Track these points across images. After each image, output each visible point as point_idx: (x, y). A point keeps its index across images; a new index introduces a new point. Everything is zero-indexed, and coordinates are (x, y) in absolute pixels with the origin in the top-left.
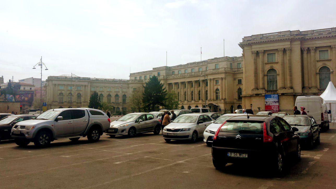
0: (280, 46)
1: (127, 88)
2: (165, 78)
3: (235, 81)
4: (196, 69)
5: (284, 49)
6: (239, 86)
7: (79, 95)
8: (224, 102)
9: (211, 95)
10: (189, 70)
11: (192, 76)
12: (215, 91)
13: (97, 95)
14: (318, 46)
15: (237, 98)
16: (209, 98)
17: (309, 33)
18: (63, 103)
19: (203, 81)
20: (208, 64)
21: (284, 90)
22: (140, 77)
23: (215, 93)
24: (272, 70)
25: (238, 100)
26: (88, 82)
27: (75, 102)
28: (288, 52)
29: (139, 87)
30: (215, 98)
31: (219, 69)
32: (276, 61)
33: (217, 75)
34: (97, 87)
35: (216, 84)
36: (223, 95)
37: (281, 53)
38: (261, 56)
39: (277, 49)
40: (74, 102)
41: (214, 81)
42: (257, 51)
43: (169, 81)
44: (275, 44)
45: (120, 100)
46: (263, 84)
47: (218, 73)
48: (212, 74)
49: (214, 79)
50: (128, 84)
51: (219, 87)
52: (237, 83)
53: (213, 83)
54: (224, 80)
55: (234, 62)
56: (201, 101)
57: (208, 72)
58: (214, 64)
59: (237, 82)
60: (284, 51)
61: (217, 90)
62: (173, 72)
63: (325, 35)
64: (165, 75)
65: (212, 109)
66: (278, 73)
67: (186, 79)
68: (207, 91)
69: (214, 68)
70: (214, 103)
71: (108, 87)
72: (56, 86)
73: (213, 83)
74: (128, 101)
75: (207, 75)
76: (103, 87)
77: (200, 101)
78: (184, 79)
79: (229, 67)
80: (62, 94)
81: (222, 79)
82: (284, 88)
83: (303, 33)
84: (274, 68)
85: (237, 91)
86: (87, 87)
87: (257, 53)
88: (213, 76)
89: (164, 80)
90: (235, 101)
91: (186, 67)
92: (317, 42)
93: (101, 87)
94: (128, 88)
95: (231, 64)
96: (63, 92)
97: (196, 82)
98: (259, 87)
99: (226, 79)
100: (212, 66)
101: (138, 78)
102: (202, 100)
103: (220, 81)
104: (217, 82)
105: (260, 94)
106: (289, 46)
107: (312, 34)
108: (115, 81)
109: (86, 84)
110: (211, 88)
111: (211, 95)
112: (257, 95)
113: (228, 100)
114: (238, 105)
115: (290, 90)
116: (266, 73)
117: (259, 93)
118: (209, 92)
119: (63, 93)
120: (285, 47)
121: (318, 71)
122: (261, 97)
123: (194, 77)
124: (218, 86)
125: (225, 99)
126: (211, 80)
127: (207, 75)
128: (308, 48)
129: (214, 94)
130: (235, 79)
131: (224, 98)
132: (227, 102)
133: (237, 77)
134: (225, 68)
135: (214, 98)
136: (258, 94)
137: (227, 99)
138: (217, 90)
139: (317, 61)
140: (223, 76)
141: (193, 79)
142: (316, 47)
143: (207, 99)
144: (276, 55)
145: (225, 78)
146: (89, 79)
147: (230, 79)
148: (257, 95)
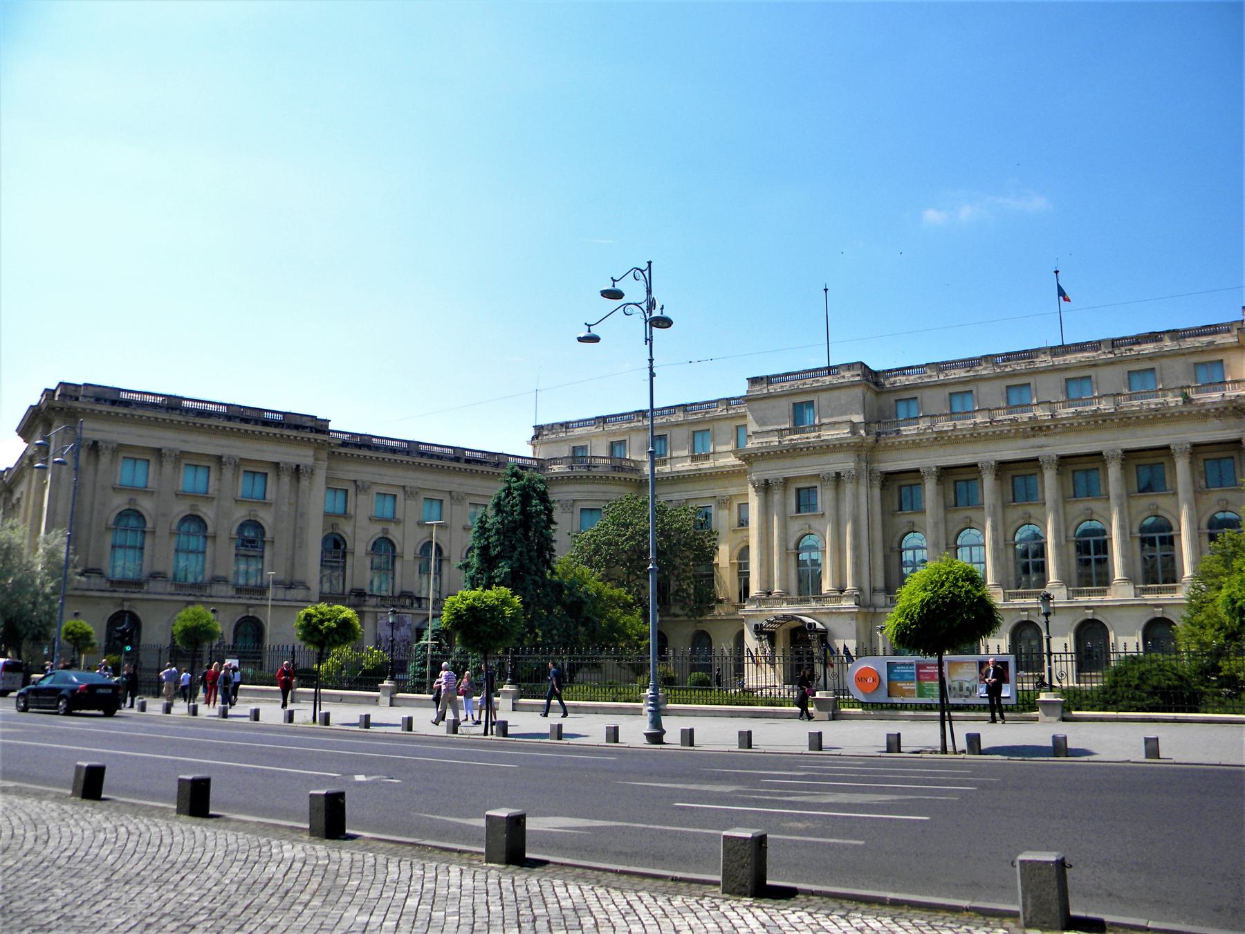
7: (249, 533)
27: (224, 580)
34: (360, 487)
72: (97, 457)
76: (392, 491)
80: (133, 522)
86: (304, 482)
93: (383, 490)
96: (146, 505)
101: (600, 449)
108: (468, 461)
109: (303, 456)
119: (140, 516)
141: (1112, 442)
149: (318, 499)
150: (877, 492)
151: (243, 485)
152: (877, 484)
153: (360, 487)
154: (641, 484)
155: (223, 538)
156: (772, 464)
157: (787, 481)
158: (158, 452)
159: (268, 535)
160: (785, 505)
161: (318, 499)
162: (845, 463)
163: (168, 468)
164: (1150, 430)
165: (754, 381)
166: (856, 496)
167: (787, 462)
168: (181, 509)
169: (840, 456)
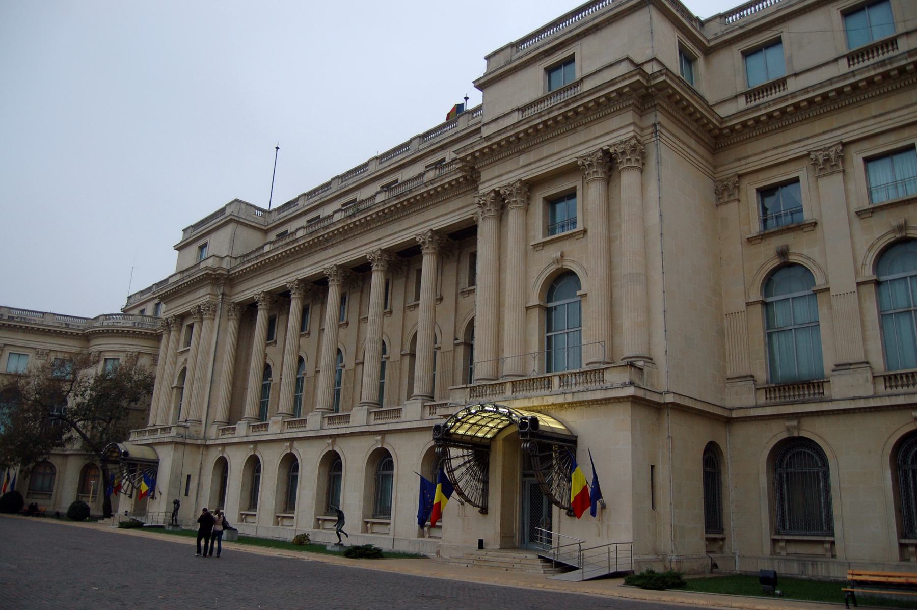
3: (731, 210)
8: (630, 391)
25: (768, 390)
35: (550, 229)
36: (628, 320)
43: (239, 288)
49: (530, 186)
52: (756, 228)
53: (526, 228)
54: (628, 180)
56: (420, 405)
59: (746, 213)
73: (526, 228)
81: (609, 163)
88: (523, 159)
90: (742, 398)
99: (643, 155)
114: (776, 433)
124: (567, 246)
126: (500, 202)
130: (725, 191)
131: (629, 347)
132: (670, 399)
133: (755, 163)
134: (639, 67)
138: (561, 280)
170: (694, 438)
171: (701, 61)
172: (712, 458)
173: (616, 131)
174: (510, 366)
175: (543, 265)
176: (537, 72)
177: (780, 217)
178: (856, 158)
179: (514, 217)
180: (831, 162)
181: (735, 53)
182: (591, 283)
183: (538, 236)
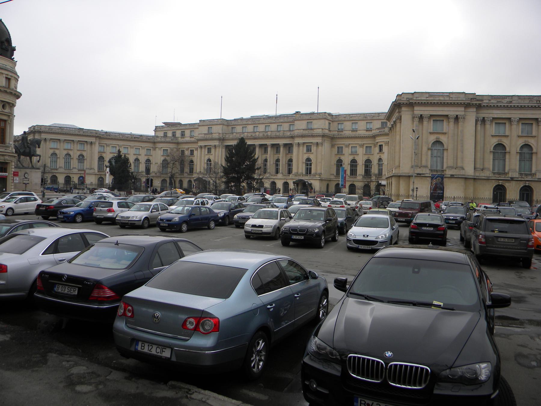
0: (452, 111)
1: (152, 149)
2: (221, 136)
4: (273, 127)
5: (457, 116)
6: (339, 156)
9: (299, 167)
10: (261, 128)
11: (268, 138)
12: (304, 161)
13: (126, 160)
14: (496, 116)
15: (335, 174)
16: (294, 170)
17: (485, 98)
18: (57, 169)
19: (285, 145)
20: (296, 122)
21: (454, 170)
22: (174, 134)
23: (304, 165)
24: (438, 142)
26: (96, 137)
28: (460, 120)
29: (172, 150)
30: (304, 173)
31: (312, 129)
32: (444, 131)
33: (309, 139)
36: (319, 168)
37: (452, 121)
38: (425, 123)
39: (447, 116)
40: (74, 168)
41: (303, 146)
42: (421, 115)
44: (446, 109)
45: (142, 168)
46: (427, 160)
47: (313, 136)
48: (303, 136)
49: (304, 143)
50: (154, 143)
51: (312, 157)
52: (336, 153)
55: (332, 121)
57: (296, 133)
58: (305, 122)
59: (335, 150)
60: (457, 118)
61: (309, 160)
62: (232, 128)
63: (505, 102)
64: (221, 132)
65: (300, 188)
66: (445, 147)
67: (256, 141)
68: (291, 160)
69: (304, 127)
70: (305, 178)
71: (111, 146)
74: (154, 168)
75: (292, 137)
77: (280, 176)
78: (254, 141)
79: (327, 128)
81: (317, 144)
82: (452, 167)
83: (478, 98)
84: (441, 140)
85: (335, 163)
86: (93, 146)
87: (421, 117)
88: (303, 139)
89: (219, 139)
90: (332, 177)
91: (257, 122)
92: (495, 111)
94: (155, 149)
95: (329, 123)
96: (57, 152)
97: (273, 145)
98: (419, 165)
100: (301, 125)
102: (282, 173)
103: (314, 149)
104: (309, 150)
105: (423, 174)
106: (463, 113)
107: (490, 100)
110: (299, 156)
111: (299, 167)
112: (419, 175)
113: (324, 176)
115: (461, 171)
116: (430, 146)
117: (421, 172)
118: (294, 163)
120: (458, 113)
121: (492, 149)
122: (423, 178)
123: (272, 138)
125: (320, 175)
126: (299, 144)
127: (292, 137)
128: (484, 118)
129: (303, 166)
130: (333, 146)
131: (319, 172)
135: (302, 170)
136: (420, 174)
137: (322, 173)
138: (309, 160)
139: (492, 136)
140: (319, 140)
142: (493, 118)
143: (290, 171)
144: (445, 123)
145: (322, 144)
146: (96, 132)
147: (327, 145)
148: (419, 175)
149: (96, 148)
150: (224, 150)
151: (79, 147)
152: (224, 148)
153: (107, 145)
154: (178, 143)
155: (75, 159)
156: (202, 142)
157: (205, 146)
158: (59, 140)
159: (85, 158)
160: (205, 151)
161: (96, 148)
162: (217, 143)
163: (62, 144)
164: (276, 140)
165: (200, 121)
166: (219, 151)
167: (206, 142)
168: (65, 152)
169: (215, 141)
170: (325, 184)
171: (331, 124)
172: (328, 185)
173: (319, 140)
174: (300, 171)
175: (306, 156)
176: (305, 122)
177: (340, 150)
178: (351, 146)
179: (301, 148)
180: (347, 146)
181: (337, 123)
182: (313, 161)
183: (305, 151)
